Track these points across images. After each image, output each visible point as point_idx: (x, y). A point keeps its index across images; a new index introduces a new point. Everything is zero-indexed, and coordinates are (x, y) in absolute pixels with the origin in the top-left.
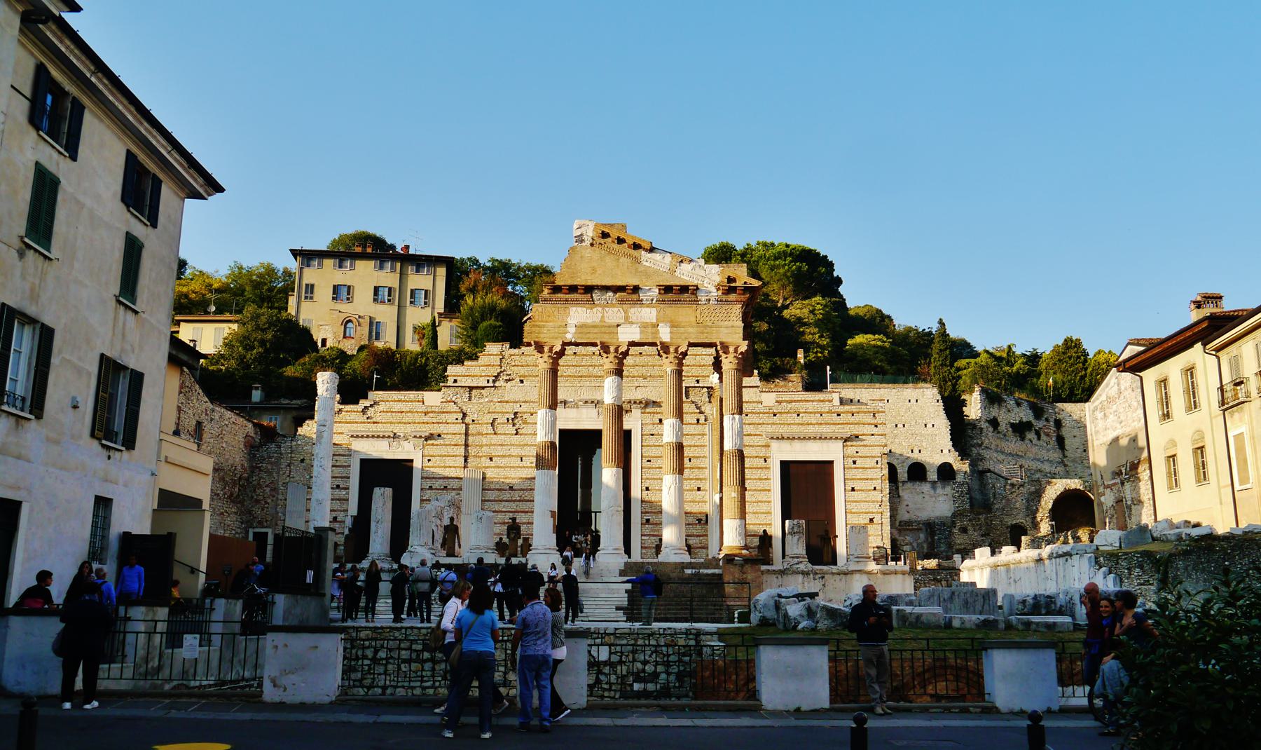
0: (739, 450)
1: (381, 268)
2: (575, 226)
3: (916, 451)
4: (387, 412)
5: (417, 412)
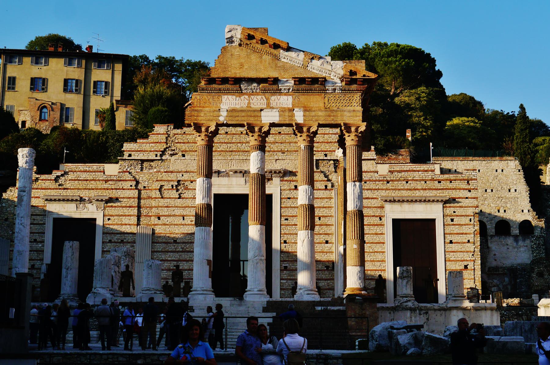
0: (359, 211)
1: (70, 64)
2: (227, 30)
3: (502, 211)
4: (75, 180)
5: (99, 180)
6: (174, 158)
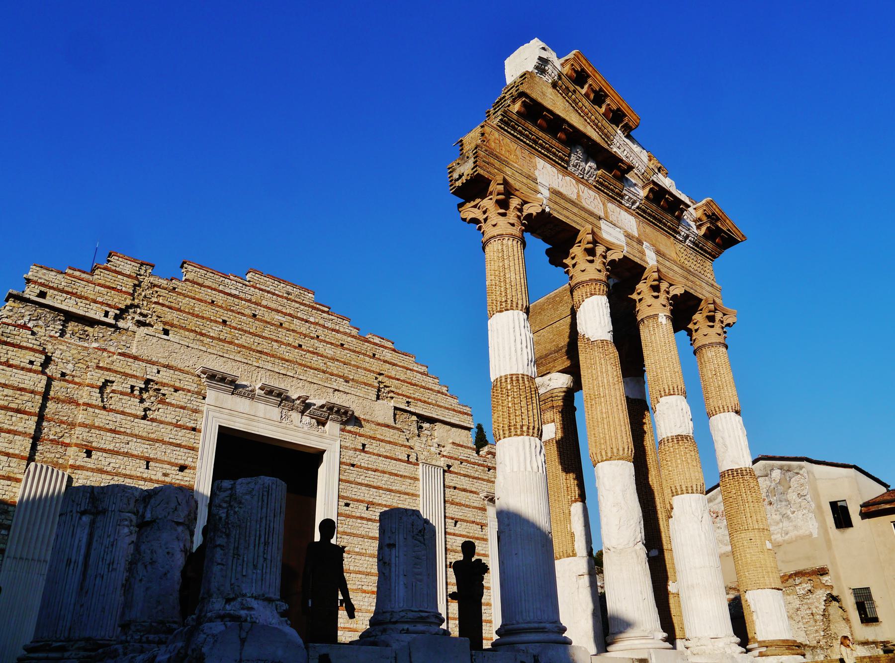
6: (143, 330)
